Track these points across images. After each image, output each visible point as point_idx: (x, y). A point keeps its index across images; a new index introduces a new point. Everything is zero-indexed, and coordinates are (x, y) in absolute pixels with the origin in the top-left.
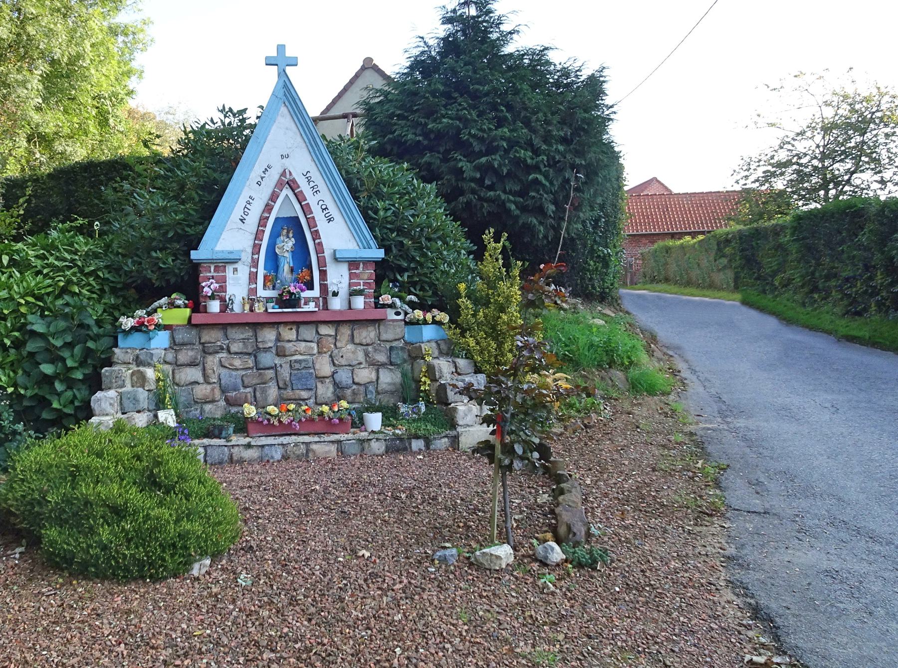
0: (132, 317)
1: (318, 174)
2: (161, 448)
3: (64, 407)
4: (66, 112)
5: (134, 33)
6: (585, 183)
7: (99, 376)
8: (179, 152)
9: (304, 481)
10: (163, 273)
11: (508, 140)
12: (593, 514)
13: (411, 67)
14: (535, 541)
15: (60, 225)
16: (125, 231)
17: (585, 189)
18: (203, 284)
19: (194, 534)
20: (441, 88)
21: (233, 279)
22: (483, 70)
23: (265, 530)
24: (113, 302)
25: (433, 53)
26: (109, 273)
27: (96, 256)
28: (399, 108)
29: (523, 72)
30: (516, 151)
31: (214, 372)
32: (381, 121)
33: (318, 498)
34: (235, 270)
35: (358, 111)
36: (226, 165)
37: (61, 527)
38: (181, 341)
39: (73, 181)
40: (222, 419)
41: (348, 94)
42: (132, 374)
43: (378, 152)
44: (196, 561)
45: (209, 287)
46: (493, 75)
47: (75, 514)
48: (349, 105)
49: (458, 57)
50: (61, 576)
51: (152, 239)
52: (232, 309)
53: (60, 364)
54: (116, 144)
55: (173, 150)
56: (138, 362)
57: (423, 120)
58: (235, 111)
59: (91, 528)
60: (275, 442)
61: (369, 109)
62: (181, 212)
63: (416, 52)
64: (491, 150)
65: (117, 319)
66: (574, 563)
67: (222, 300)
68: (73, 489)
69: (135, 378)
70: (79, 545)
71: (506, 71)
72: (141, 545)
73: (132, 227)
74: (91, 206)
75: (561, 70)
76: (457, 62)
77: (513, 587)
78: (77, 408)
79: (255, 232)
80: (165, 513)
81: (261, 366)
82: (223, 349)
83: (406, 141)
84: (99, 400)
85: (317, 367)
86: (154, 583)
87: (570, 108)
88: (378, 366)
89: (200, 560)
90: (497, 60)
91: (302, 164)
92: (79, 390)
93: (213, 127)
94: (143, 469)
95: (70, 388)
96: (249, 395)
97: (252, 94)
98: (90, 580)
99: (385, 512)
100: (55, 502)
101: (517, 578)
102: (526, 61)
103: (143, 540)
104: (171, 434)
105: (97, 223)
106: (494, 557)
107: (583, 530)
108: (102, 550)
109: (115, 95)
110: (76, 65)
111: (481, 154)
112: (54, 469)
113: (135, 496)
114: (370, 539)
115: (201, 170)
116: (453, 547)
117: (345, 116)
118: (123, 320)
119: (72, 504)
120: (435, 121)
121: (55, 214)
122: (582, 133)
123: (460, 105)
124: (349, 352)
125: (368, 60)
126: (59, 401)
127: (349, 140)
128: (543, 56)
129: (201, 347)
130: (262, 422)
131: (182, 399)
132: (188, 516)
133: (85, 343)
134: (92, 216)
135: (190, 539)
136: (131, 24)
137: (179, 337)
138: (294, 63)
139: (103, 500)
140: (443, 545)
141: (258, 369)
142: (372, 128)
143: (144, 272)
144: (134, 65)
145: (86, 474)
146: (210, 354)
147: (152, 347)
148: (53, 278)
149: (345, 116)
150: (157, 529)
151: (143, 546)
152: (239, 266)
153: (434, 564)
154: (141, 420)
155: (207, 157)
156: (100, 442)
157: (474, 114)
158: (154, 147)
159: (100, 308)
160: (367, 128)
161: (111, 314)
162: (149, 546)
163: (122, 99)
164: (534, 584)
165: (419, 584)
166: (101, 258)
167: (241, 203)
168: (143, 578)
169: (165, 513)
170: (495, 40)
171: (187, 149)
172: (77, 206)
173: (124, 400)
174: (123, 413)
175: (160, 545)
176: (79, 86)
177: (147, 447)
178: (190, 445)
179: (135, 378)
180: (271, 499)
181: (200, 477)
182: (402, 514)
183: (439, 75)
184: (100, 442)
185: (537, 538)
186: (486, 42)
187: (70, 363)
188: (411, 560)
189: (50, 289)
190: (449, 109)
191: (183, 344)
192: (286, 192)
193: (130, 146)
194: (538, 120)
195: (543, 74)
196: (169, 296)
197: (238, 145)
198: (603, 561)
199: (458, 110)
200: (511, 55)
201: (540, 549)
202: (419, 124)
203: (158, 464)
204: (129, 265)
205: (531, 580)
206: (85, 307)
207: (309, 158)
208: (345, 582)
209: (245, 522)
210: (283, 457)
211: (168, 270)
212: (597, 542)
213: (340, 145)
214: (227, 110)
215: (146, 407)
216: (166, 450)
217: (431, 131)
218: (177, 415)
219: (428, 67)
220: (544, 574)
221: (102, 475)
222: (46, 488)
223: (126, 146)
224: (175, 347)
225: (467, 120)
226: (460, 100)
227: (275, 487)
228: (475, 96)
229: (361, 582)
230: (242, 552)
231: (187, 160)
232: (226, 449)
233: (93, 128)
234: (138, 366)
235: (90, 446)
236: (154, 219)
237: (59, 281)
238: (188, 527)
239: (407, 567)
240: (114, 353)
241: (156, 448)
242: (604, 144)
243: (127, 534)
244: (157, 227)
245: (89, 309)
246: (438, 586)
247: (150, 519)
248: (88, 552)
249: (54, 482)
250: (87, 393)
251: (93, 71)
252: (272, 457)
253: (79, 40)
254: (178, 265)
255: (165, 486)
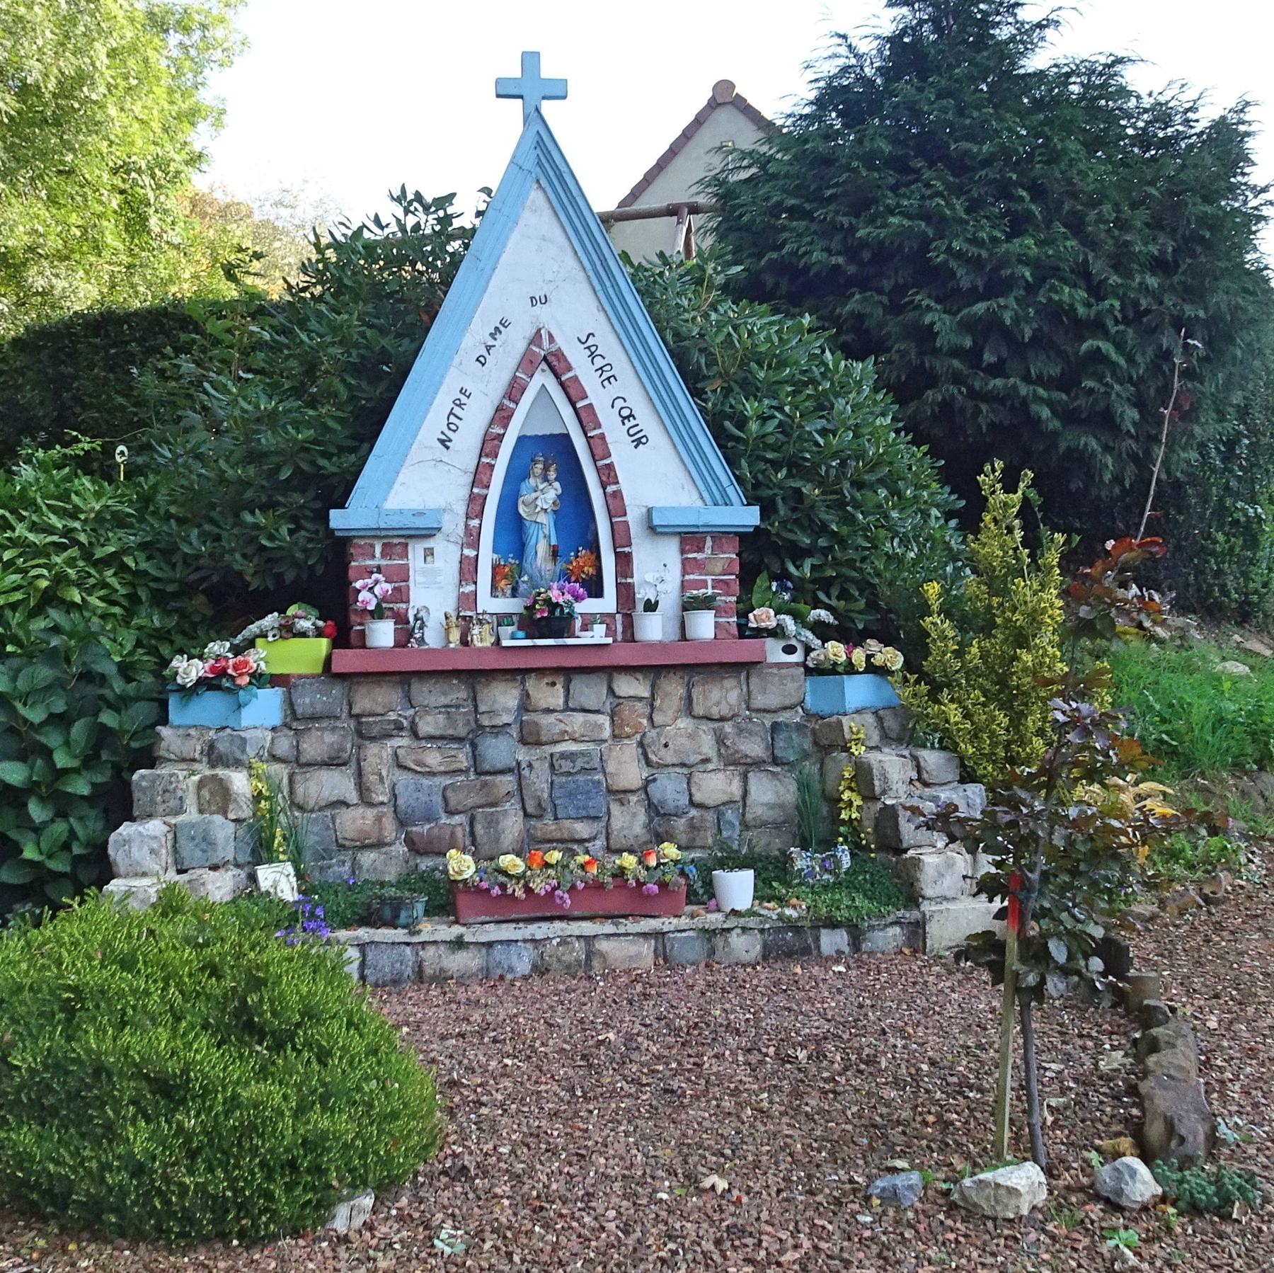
0: (201, 657)
1: (612, 338)
2: (263, 949)
3: (50, 857)
4: (52, 201)
5: (204, 27)
6: (1205, 360)
7: (126, 787)
8: (304, 290)
9: (581, 1021)
10: (268, 559)
11: (1035, 264)
12: (1223, 1095)
13: (820, 102)
14: (1094, 1156)
15: (40, 454)
16: (185, 465)
17: (1206, 372)
18: (358, 584)
19: (337, 1139)
20: (886, 148)
21: (424, 573)
22: (978, 107)
23: (494, 1131)
24: (157, 624)
25: (868, 71)
26: (149, 558)
27: (120, 521)
28: (794, 193)
29: (1067, 113)
30: (1053, 289)
31: (381, 779)
32: (752, 221)
33: (612, 1060)
34: (429, 553)
35: (702, 200)
36: (409, 319)
37: (43, 1124)
38: (309, 711)
39: (69, 355)
40: (399, 885)
41: (679, 161)
42: (201, 785)
43: (746, 291)
44: (341, 1200)
45: (371, 590)
46: (1001, 119)
47: (73, 1096)
48: (681, 186)
49: (924, 79)
50: (42, 1233)
51: (245, 484)
52: (422, 641)
53: (39, 762)
54: (164, 274)
55: (290, 287)
56: (214, 756)
57: (845, 221)
58: (429, 199)
59: (108, 1126)
60: (518, 935)
61: (726, 195)
62: (309, 424)
63: (832, 68)
64: (996, 287)
65: (165, 663)
66: (1181, 1204)
67: (401, 619)
68: (69, 1039)
69: (205, 793)
70: (82, 1164)
71: (1030, 111)
72: (220, 1163)
73: (199, 457)
74: (109, 411)
75: (1152, 109)
76: (920, 90)
77: (1046, 1256)
78: (77, 861)
79: (473, 469)
80: (272, 1092)
81: (487, 767)
82: (401, 728)
83: (807, 268)
84: (127, 842)
85: (610, 768)
86: (247, 1248)
87: (1171, 193)
88: (745, 766)
89: (350, 1197)
90: (1011, 85)
91: (577, 317)
92: (81, 819)
93: (380, 235)
94: (225, 996)
95: (61, 814)
96: (459, 831)
97: (466, 161)
98: (107, 1241)
99: (762, 1090)
100: (29, 1069)
101: (1053, 1238)
102: (1075, 89)
103: (224, 1153)
104: (287, 918)
105: (121, 448)
106: (1002, 1192)
107: (1202, 1130)
108: (133, 1176)
109: (161, 163)
110: (75, 98)
111: (975, 295)
112: (26, 995)
113: (205, 1056)
114: (728, 1152)
115: (354, 331)
116: (913, 1168)
117: (672, 211)
118: (179, 663)
119: (67, 1073)
120: (871, 221)
121: (29, 428)
122: (1199, 249)
123: (928, 185)
124: (682, 734)
125: (724, 87)
126: (38, 844)
127: (682, 264)
128: (1111, 76)
129: (352, 724)
130: (488, 890)
131: (311, 840)
132: (324, 1099)
133: (96, 715)
134: (110, 432)
135: (329, 1150)
136: (197, 6)
137: (304, 702)
138: (558, 92)
139: (136, 1065)
140: (890, 1163)
141: (479, 773)
142: (732, 237)
143: (227, 557)
144: (205, 96)
145: (97, 1007)
146: (373, 739)
147: (244, 723)
148: (24, 571)
149: (672, 211)
150: (255, 1128)
151: (224, 1165)
152: (436, 543)
153: (870, 1207)
154: (220, 887)
155: (365, 302)
156: (129, 936)
157: (959, 205)
158: (249, 280)
159: (128, 638)
160: (721, 238)
161: (153, 651)
162: (237, 1166)
163: (178, 172)
164: (1093, 1251)
165: (836, 1250)
166: (131, 526)
167: (443, 403)
168: (224, 1237)
169: (272, 1092)
170: (1006, 43)
171: (322, 283)
172: (78, 410)
173: (182, 841)
174: (180, 872)
175: (263, 1164)
176: (83, 144)
177: (233, 946)
178: (328, 942)
179: (205, 793)
180: (508, 1062)
181: (350, 1014)
182: (800, 1096)
183: (882, 120)
184: (129, 936)
185: (1098, 1150)
186: (987, 47)
187: (61, 760)
188: (819, 1198)
189: (18, 596)
190: (904, 196)
191: (314, 718)
192: (543, 378)
193: (196, 276)
194: (1100, 219)
195: (1111, 118)
196: (282, 611)
197: (436, 276)
198: (1246, 1199)
199: (923, 197)
200: (1041, 75)
201: (1105, 1173)
202: (835, 228)
203: (258, 984)
204: (194, 543)
205: (1086, 1241)
206: (95, 636)
207: (593, 304)
208: (671, 1246)
209: (451, 1112)
210: (535, 968)
211: (279, 554)
212: (1231, 1158)
213: (661, 274)
214: (410, 196)
215: (230, 857)
216: (274, 952)
217: (864, 243)
218: (299, 875)
219: (858, 102)
220: (1114, 1229)
221: (134, 1008)
222: (8, 1037)
223: (185, 278)
224: (295, 725)
225: (943, 218)
226: (927, 174)
227: (517, 1035)
228: (961, 166)
229: (708, 1246)
230: (444, 1179)
231: (323, 307)
232: (408, 950)
233: (112, 236)
234: (213, 767)
235: (106, 944)
236: (248, 440)
237: (38, 577)
238: (325, 1123)
239: (810, 1213)
240: (159, 737)
241: (252, 949)
242: (1248, 273)
243: (188, 1140)
244: (254, 457)
245: (103, 640)
246: (879, 1256)
247: (239, 1106)
248: (103, 1180)
249: (27, 1024)
250: (100, 825)
251: (113, 111)
252: (511, 969)
253: (82, 42)
254: (302, 542)
255: (273, 1033)
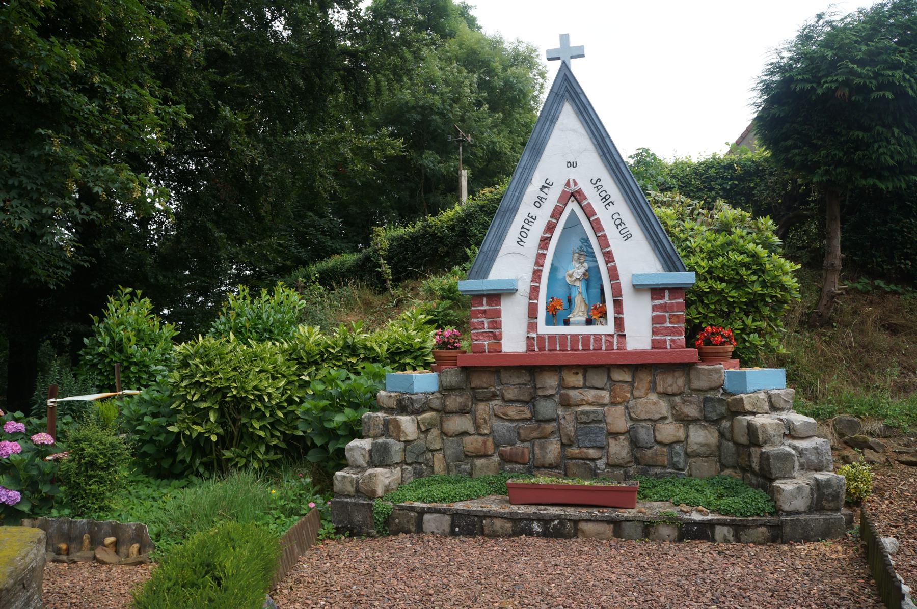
81: (540, 417)
85: (609, 420)
88: (686, 421)
96: (526, 451)
124: (651, 404)
141: (539, 421)
146: (482, 401)
